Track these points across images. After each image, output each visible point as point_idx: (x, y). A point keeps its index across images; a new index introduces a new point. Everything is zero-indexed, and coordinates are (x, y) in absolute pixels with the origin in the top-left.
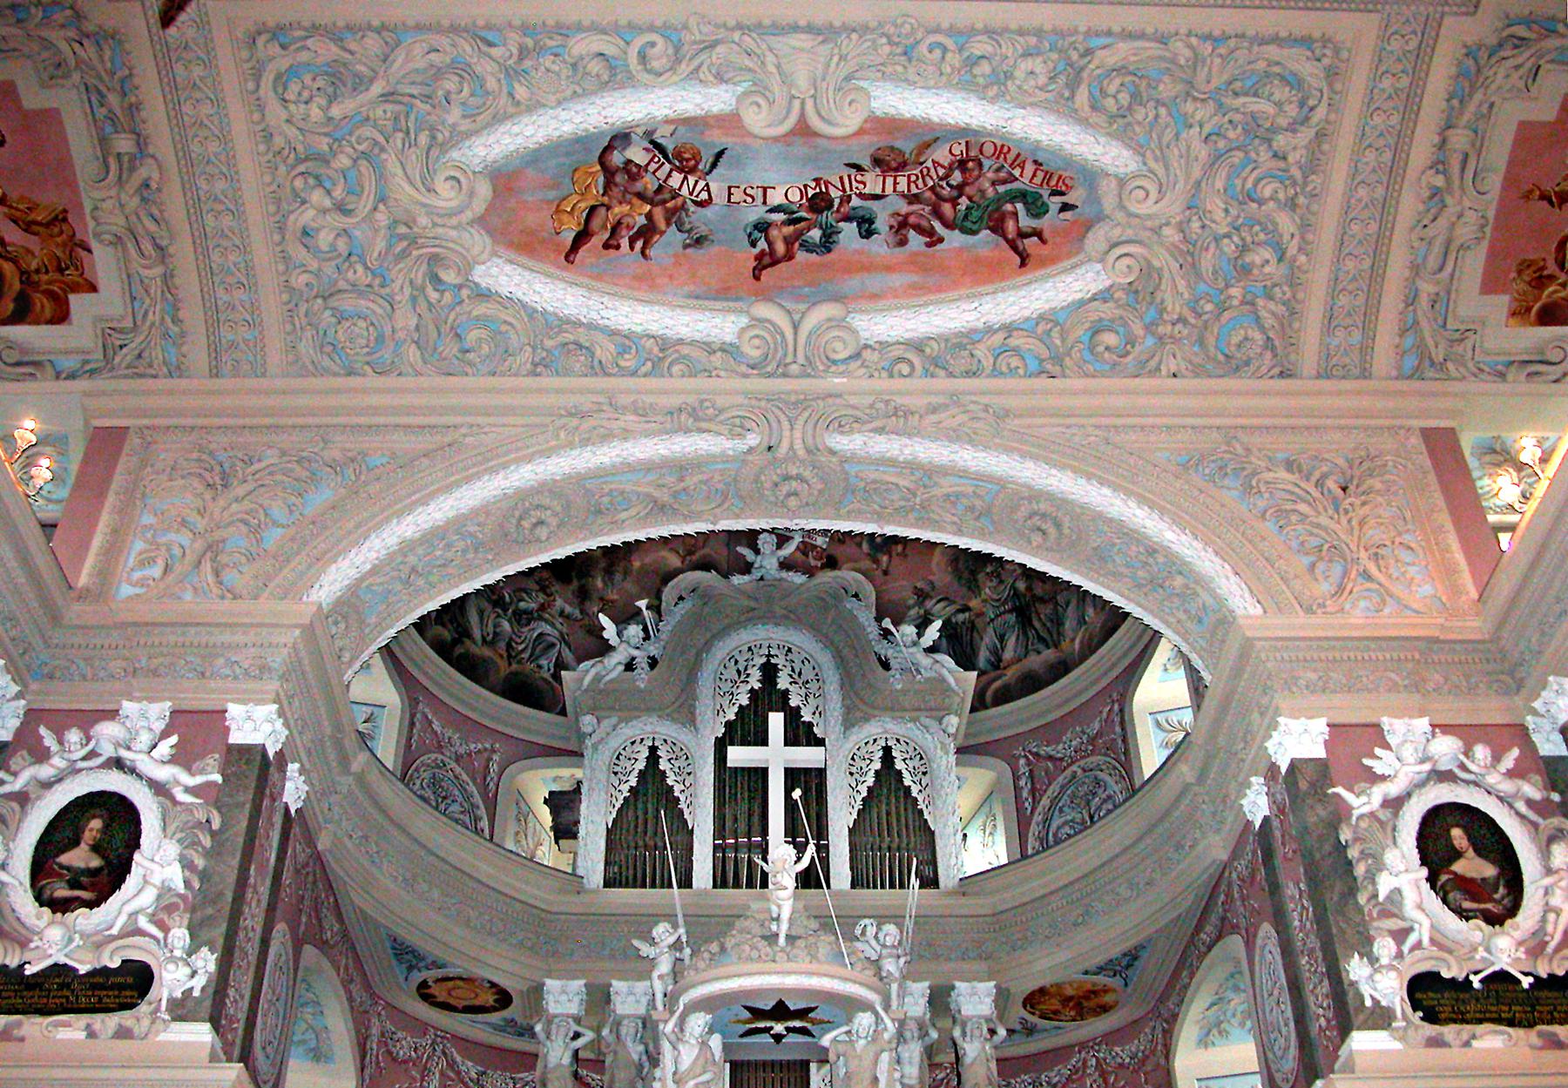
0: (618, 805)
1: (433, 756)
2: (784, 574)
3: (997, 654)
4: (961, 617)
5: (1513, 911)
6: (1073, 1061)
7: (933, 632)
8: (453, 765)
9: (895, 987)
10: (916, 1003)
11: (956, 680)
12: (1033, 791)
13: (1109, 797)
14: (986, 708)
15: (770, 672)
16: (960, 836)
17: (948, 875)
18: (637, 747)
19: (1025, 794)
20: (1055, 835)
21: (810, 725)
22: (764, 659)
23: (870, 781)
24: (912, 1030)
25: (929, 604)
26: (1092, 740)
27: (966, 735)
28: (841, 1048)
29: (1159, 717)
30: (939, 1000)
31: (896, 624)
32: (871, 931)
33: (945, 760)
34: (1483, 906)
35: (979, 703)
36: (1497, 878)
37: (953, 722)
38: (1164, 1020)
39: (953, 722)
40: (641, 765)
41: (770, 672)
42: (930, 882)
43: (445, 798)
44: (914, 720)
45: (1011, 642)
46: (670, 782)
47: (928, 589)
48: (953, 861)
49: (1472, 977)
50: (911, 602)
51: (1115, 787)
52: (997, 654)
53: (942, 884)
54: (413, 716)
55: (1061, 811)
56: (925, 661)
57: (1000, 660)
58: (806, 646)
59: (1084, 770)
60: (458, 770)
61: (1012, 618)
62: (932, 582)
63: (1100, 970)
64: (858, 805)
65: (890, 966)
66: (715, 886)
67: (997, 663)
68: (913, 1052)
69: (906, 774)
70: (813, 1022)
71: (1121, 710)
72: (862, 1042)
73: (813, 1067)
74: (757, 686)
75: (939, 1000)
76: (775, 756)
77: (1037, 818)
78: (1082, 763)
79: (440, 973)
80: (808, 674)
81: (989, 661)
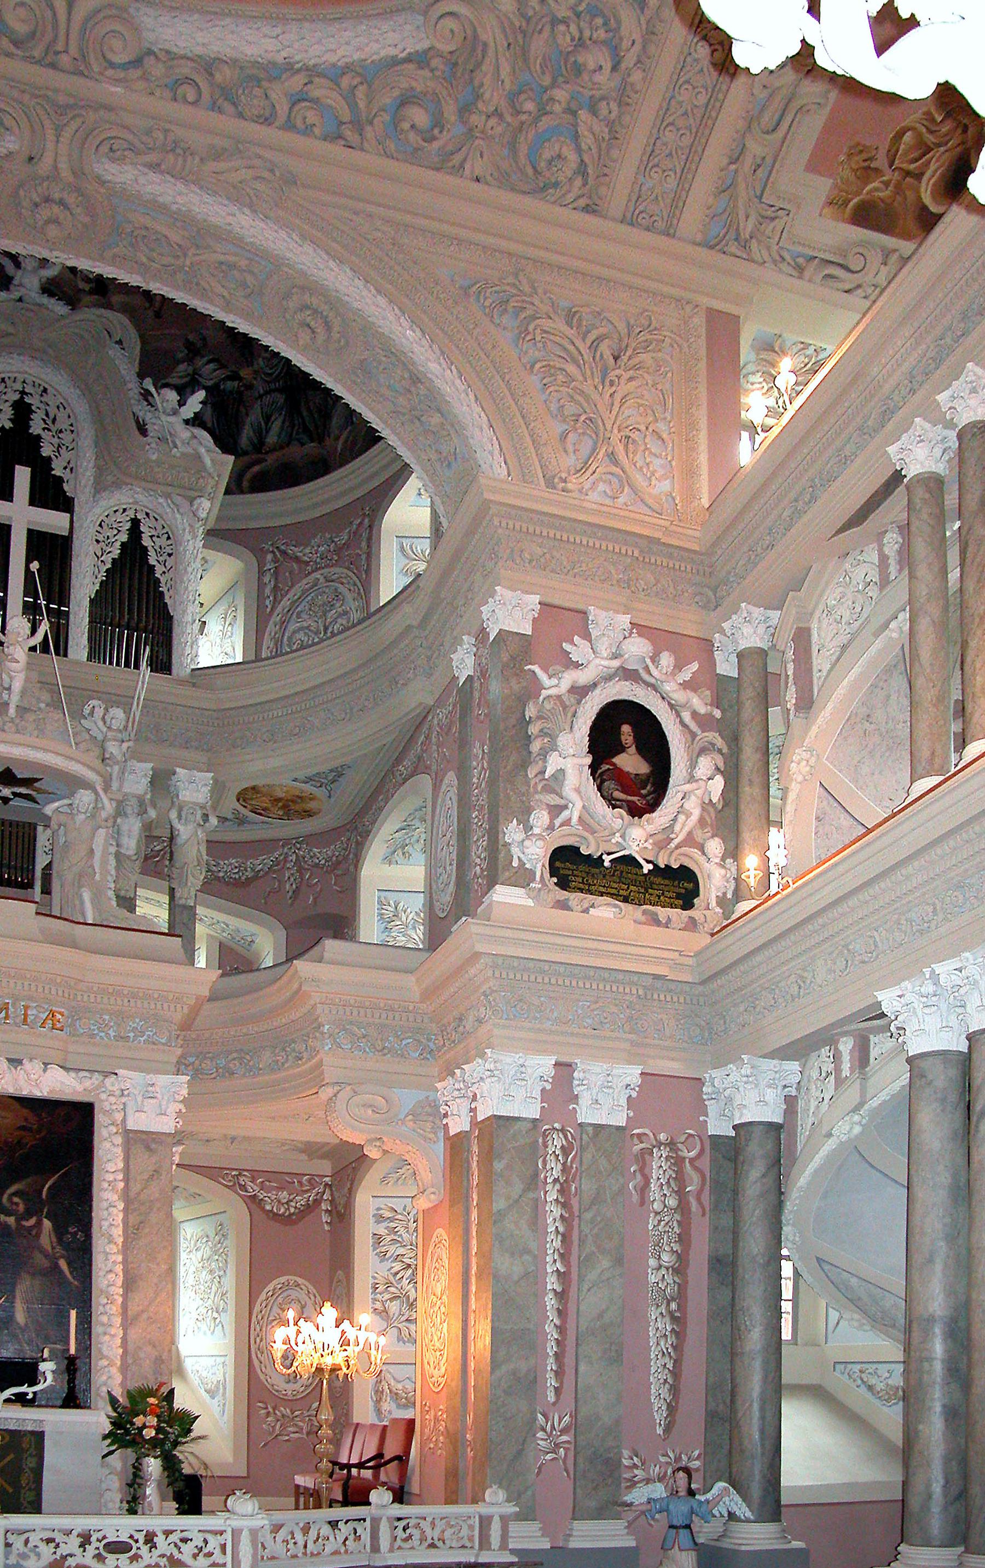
2: (45, 300)
3: (261, 435)
4: (230, 385)
5: (652, 806)
9: (116, 768)
10: (137, 781)
11: (212, 460)
12: (276, 588)
13: (345, 613)
14: (242, 492)
16: (197, 625)
17: (183, 663)
19: (267, 591)
20: (290, 638)
21: (60, 480)
23: (116, 553)
24: (131, 807)
25: (200, 362)
26: (339, 550)
27: (219, 518)
28: (63, 818)
30: (161, 781)
32: (99, 712)
33: (193, 545)
34: (630, 798)
35: (235, 486)
36: (648, 776)
37: (205, 506)
38: (355, 832)
39: (205, 506)
42: (162, 664)
44: (167, 496)
45: (276, 426)
47: (199, 344)
49: (604, 857)
50: (180, 355)
51: (352, 604)
52: (261, 435)
53: (174, 671)
55: (299, 616)
56: (185, 433)
57: (262, 443)
61: (280, 399)
62: (204, 339)
63: (308, 780)
64: (102, 576)
65: (113, 748)
67: (259, 446)
68: (132, 828)
70: (38, 790)
72: (82, 817)
73: (40, 829)
75: (161, 781)
81: (250, 440)
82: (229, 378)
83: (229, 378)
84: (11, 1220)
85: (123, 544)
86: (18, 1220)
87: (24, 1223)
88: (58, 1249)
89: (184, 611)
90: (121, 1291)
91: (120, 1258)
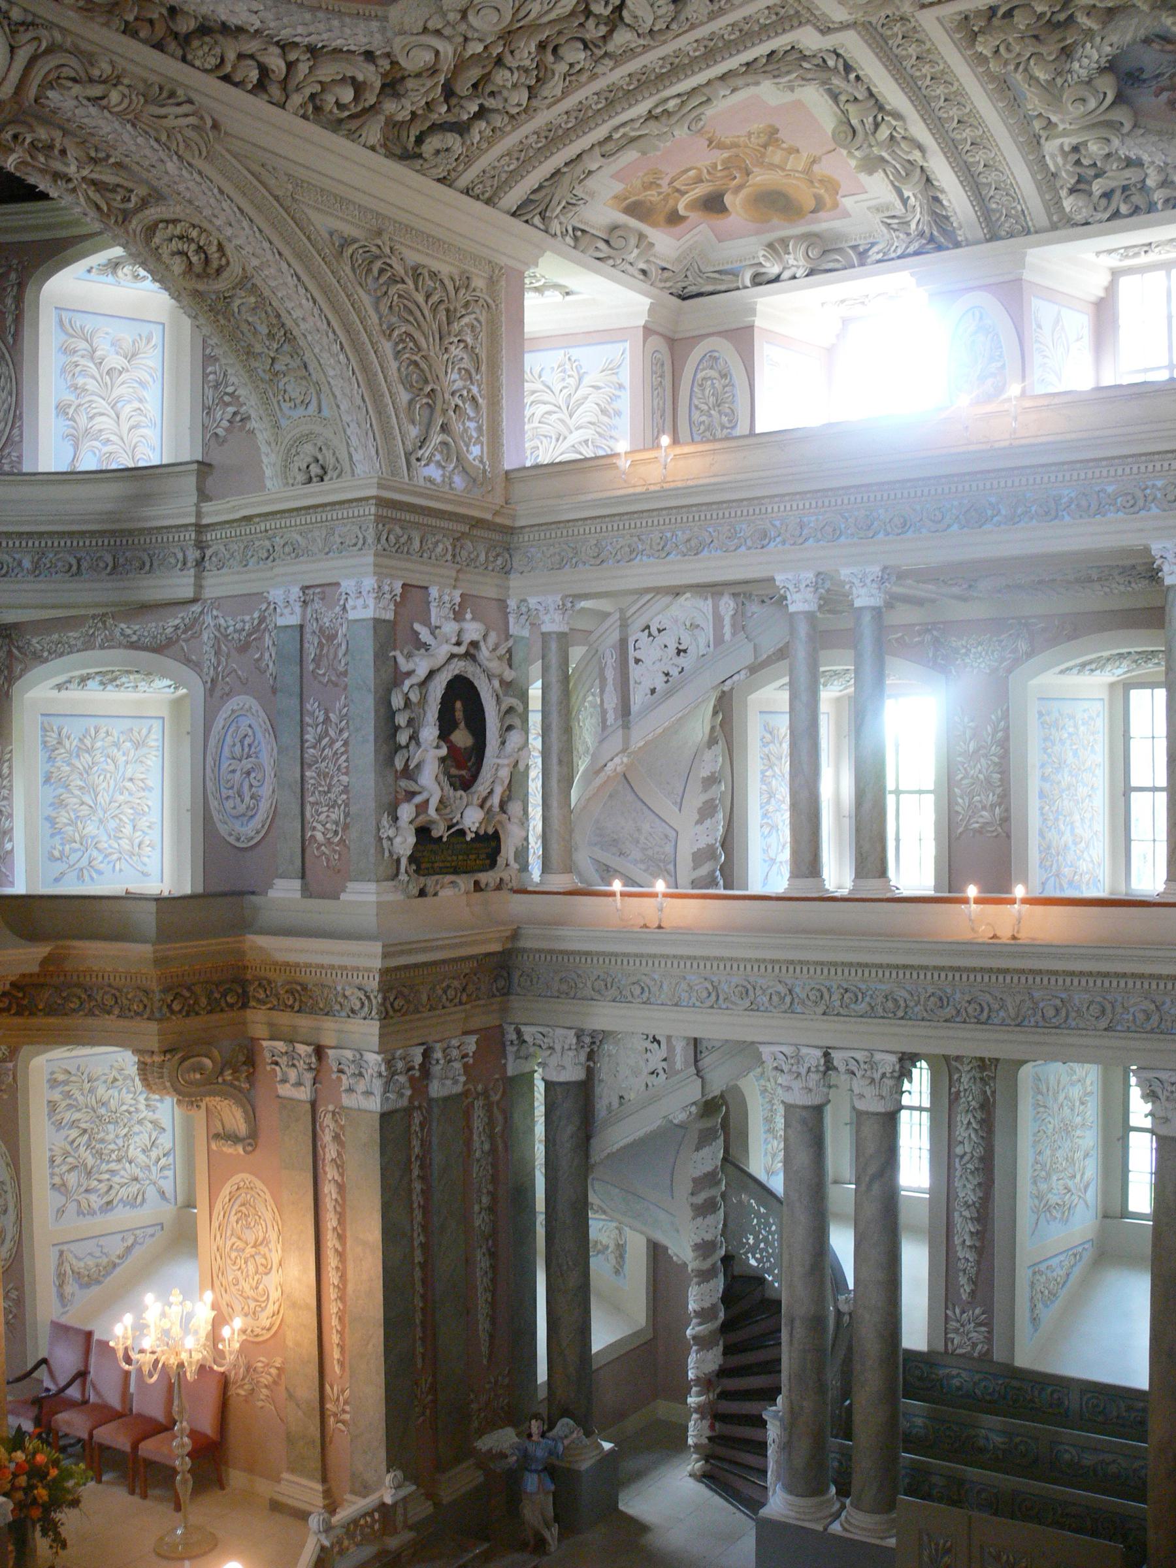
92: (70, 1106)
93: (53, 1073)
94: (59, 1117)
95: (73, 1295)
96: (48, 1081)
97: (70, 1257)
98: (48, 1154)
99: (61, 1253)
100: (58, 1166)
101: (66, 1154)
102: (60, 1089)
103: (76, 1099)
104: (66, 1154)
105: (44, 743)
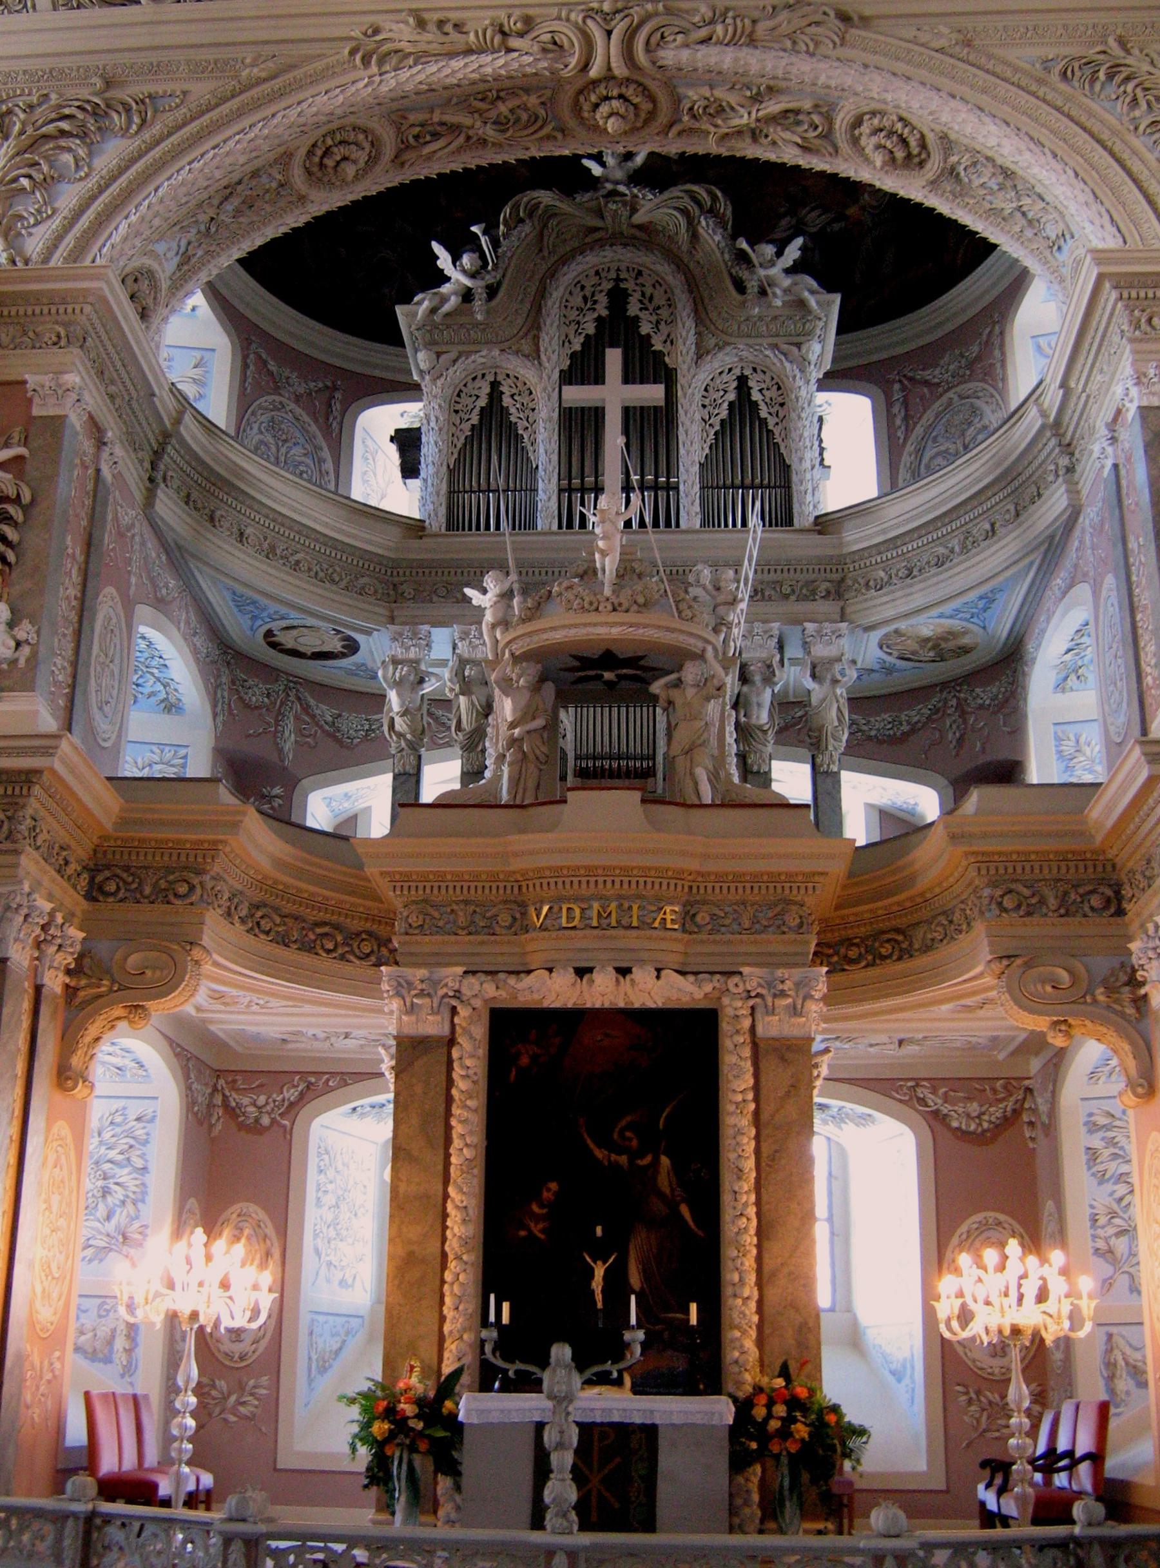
0: (459, 445)
1: (271, 398)
4: (836, 227)
6: (934, 701)
7: (793, 252)
8: (292, 406)
15: (618, 297)
17: (805, 514)
18: (478, 383)
22: (610, 285)
29: (1041, 341)
31: (752, 244)
40: (482, 402)
41: (618, 297)
43: (285, 441)
46: (513, 419)
48: (809, 498)
53: (796, 521)
54: (245, 358)
58: (658, 268)
59: (961, 397)
60: (299, 411)
66: (560, 527)
69: (762, 406)
71: (1002, 333)
74: (605, 313)
76: (614, 394)
77: (910, 448)
78: (958, 389)
79: (284, 623)
80: (660, 299)
82: (833, 221)
83: (833, 221)
84: (623, 1159)
85: (731, 404)
86: (631, 1161)
87: (640, 1163)
88: (678, 1191)
89: (801, 460)
90: (755, 1240)
91: (753, 1198)
92: (1115, 1156)
93: (1091, 1115)
94: (1101, 1168)
95: (1128, 1393)
96: (1086, 1124)
97: (1122, 1343)
98: (1089, 1211)
99: (1110, 1336)
100: (1103, 1227)
101: (1113, 1214)
102: (1101, 1134)
103: (1122, 1148)
104: (1113, 1214)
105: (1060, 752)
